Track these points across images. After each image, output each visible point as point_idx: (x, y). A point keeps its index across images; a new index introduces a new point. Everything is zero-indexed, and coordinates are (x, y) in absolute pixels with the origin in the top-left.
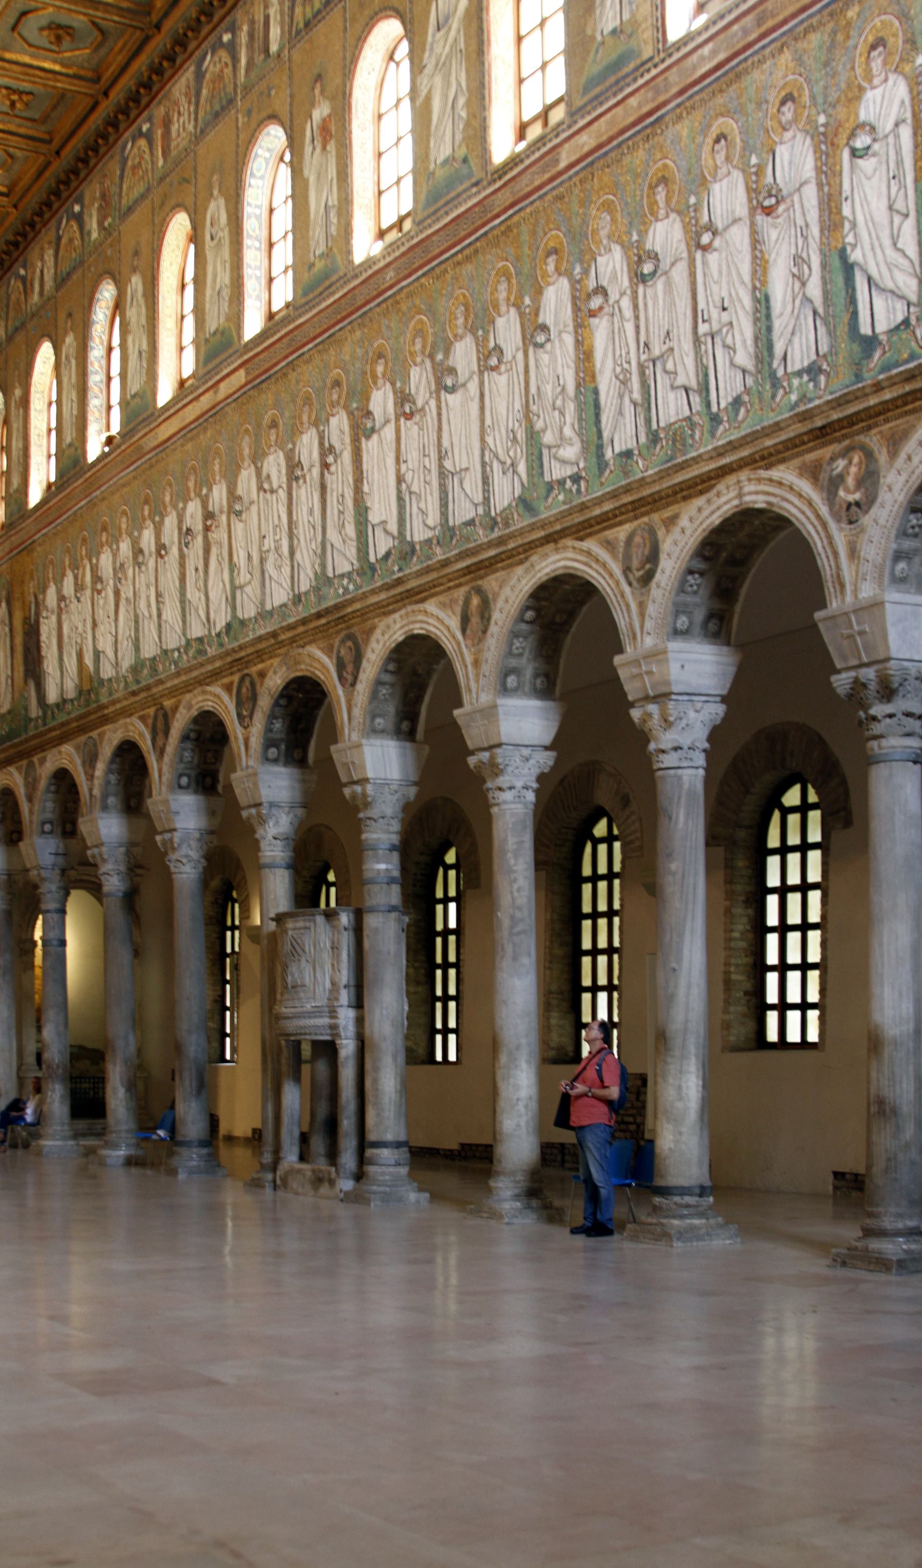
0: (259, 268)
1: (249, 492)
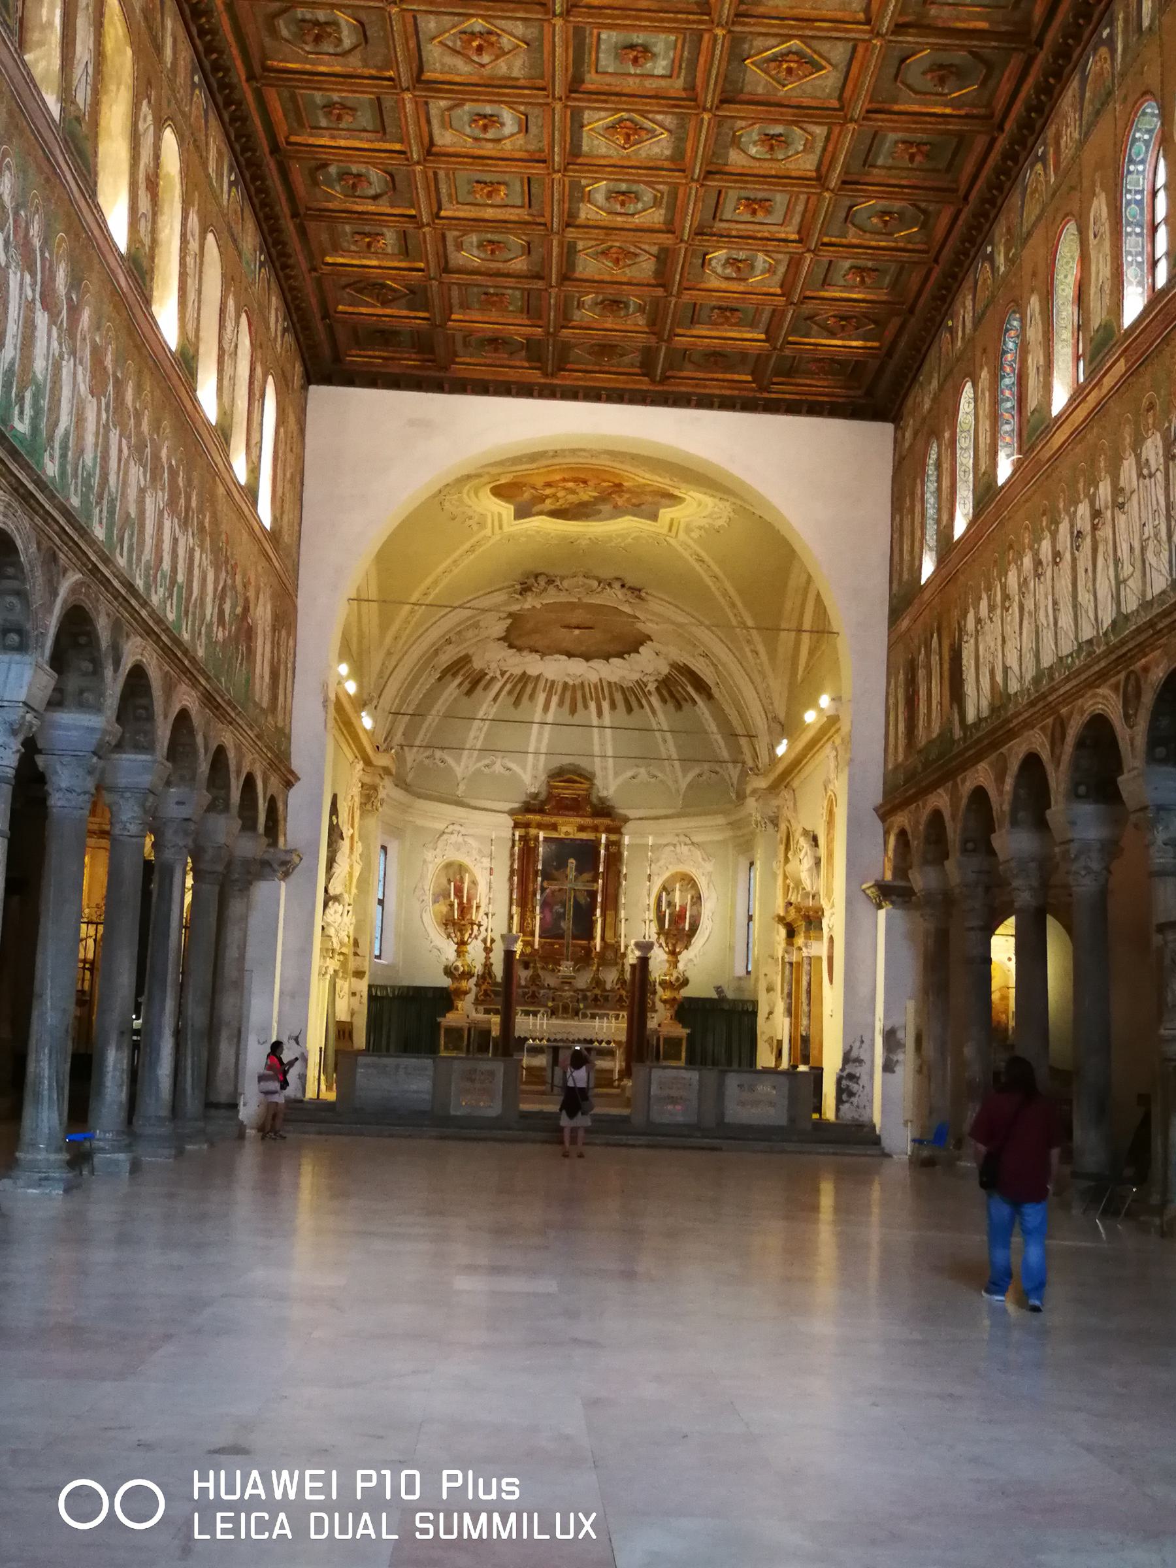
0: (1141, 254)
1: (1130, 482)
